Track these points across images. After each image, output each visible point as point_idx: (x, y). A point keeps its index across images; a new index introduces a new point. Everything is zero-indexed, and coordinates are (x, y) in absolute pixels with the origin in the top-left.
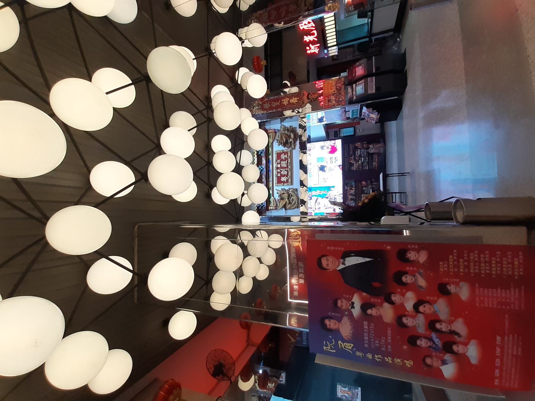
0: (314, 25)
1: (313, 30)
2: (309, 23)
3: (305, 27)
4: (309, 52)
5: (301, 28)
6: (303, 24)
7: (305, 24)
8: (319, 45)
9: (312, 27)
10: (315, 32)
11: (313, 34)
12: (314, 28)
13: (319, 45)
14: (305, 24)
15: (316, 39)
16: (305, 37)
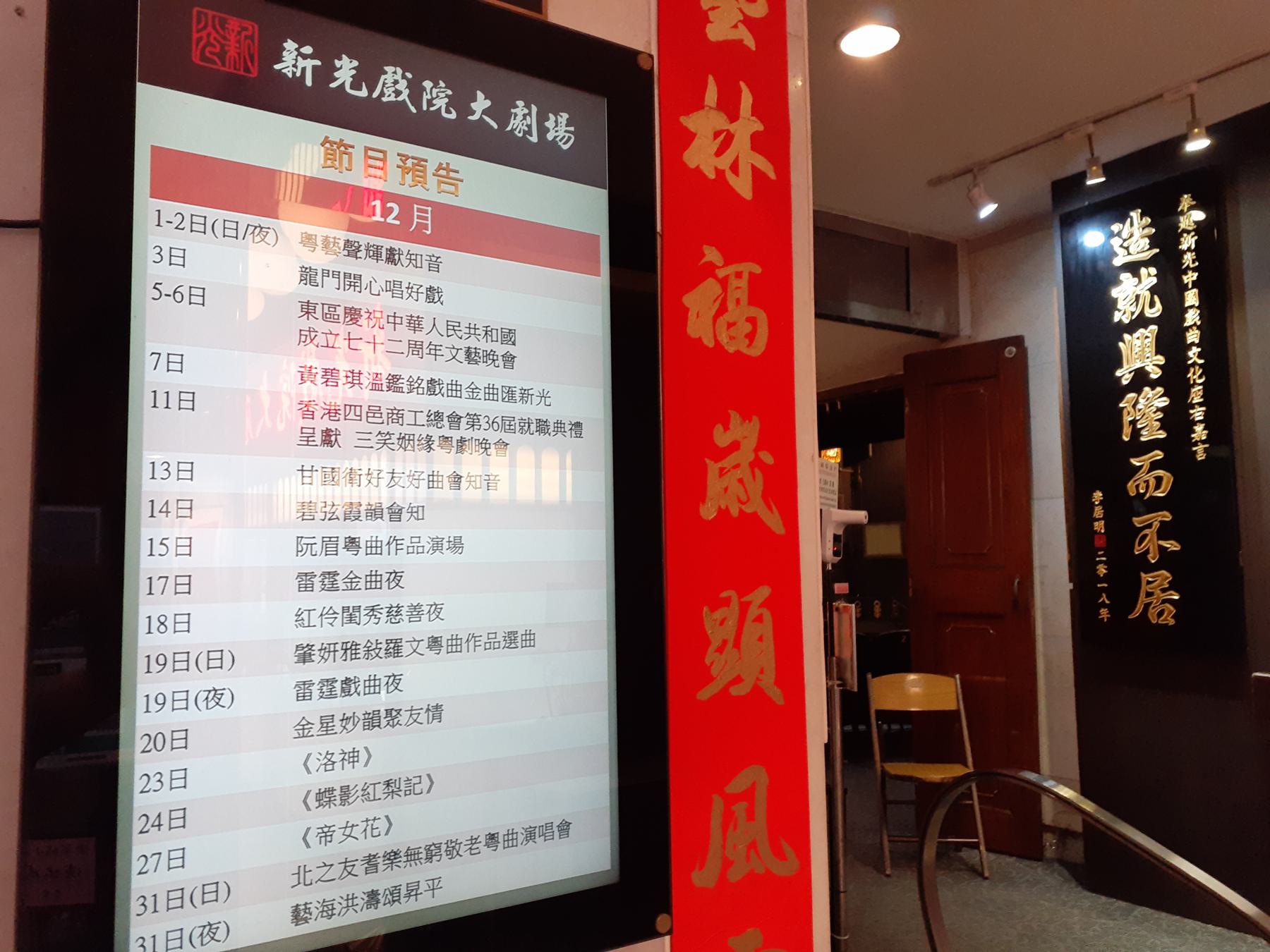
0: (385, 99)
1: (371, 91)
2: (398, 93)
4: (290, 45)
5: (390, 69)
6: (398, 77)
7: (396, 82)
8: (309, 82)
9: (382, 94)
10: (364, 93)
11: (356, 85)
12: (375, 95)
13: (309, 82)
14: (396, 82)
15: (333, 85)
16: (355, 63)
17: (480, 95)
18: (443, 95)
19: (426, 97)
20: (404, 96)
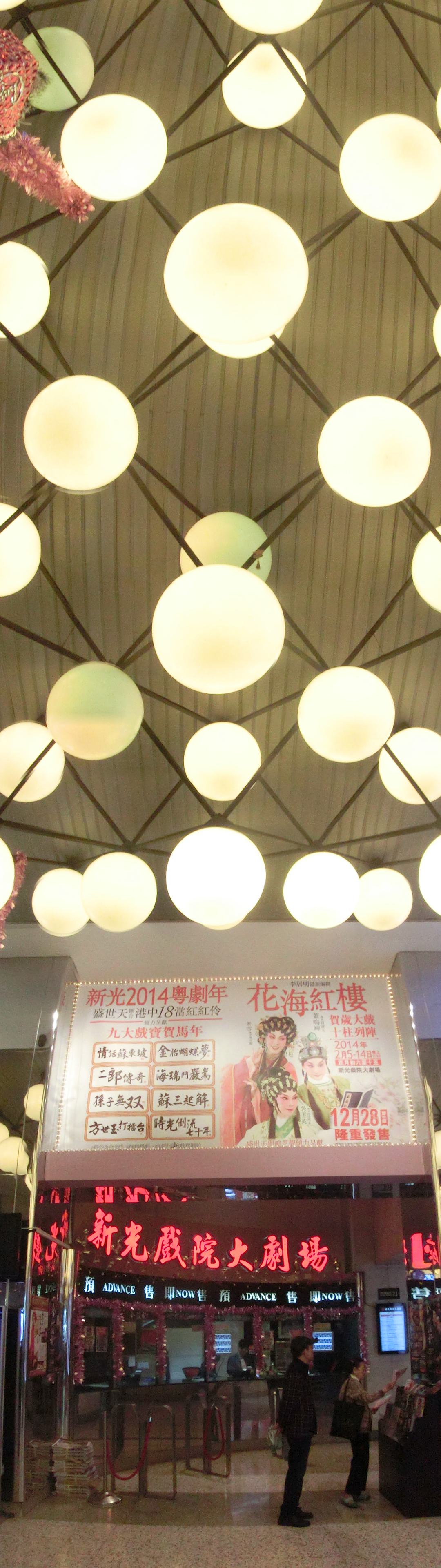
0: (163, 1261)
2: (172, 1251)
3: (164, 1240)
5: (165, 1230)
6: (172, 1236)
9: (161, 1256)
11: (140, 1252)
14: (171, 1242)
17: (238, 1242)
18: (209, 1247)
19: (196, 1251)
20: (177, 1254)
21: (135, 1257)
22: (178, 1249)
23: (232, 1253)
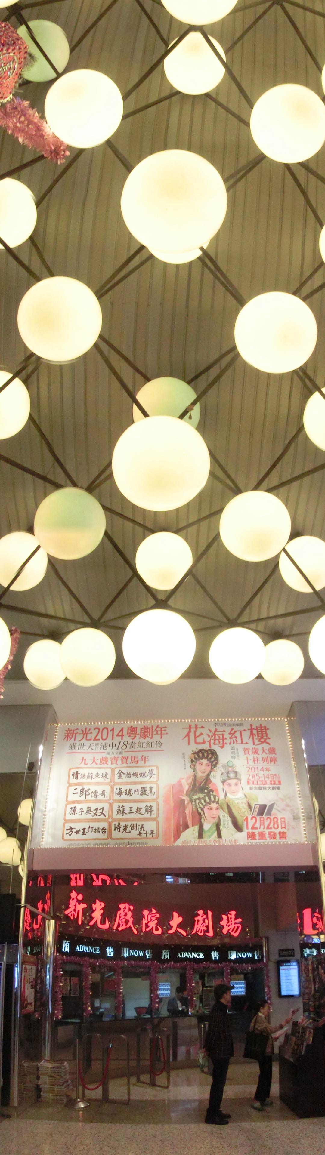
2: (127, 922)
3: (120, 913)
5: (122, 906)
6: (127, 910)
9: (119, 925)
11: (103, 922)
14: (126, 915)
17: (175, 915)
18: (154, 919)
19: (144, 922)
20: (130, 924)
21: (100, 926)
22: (131, 920)
23: (171, 923)
